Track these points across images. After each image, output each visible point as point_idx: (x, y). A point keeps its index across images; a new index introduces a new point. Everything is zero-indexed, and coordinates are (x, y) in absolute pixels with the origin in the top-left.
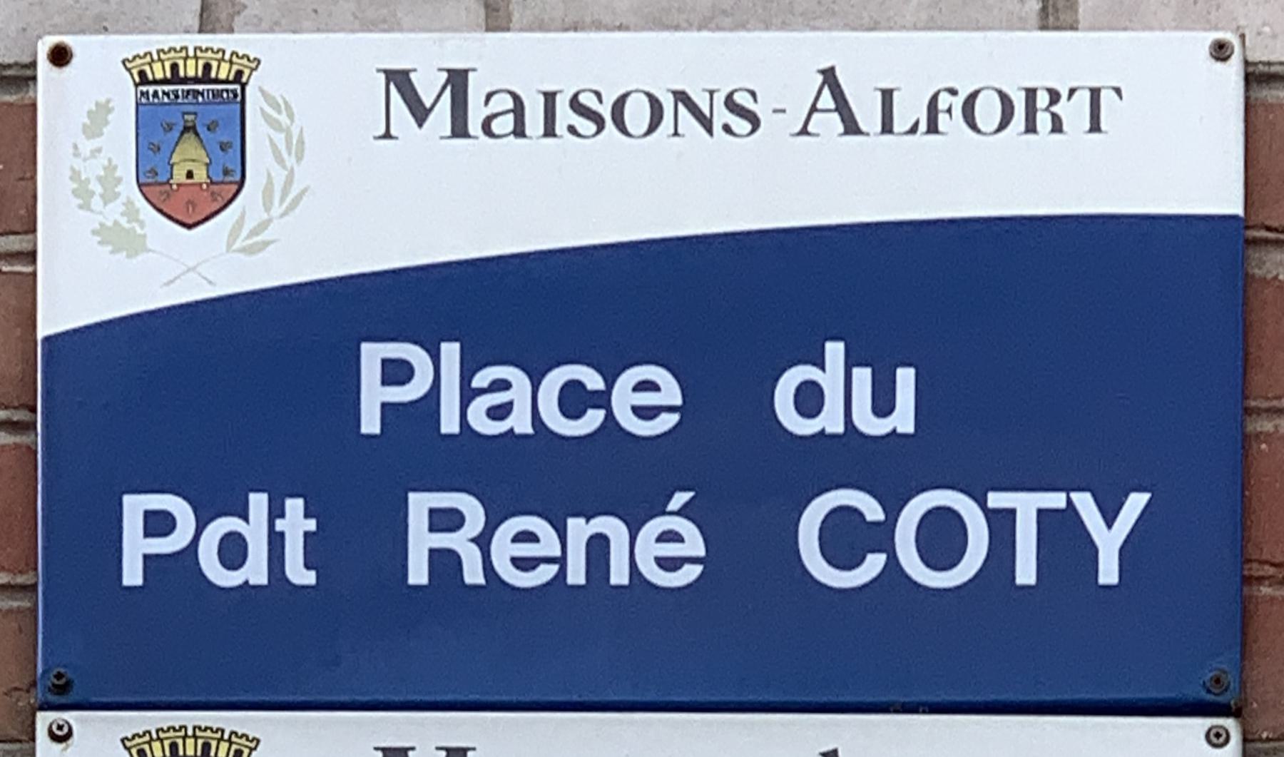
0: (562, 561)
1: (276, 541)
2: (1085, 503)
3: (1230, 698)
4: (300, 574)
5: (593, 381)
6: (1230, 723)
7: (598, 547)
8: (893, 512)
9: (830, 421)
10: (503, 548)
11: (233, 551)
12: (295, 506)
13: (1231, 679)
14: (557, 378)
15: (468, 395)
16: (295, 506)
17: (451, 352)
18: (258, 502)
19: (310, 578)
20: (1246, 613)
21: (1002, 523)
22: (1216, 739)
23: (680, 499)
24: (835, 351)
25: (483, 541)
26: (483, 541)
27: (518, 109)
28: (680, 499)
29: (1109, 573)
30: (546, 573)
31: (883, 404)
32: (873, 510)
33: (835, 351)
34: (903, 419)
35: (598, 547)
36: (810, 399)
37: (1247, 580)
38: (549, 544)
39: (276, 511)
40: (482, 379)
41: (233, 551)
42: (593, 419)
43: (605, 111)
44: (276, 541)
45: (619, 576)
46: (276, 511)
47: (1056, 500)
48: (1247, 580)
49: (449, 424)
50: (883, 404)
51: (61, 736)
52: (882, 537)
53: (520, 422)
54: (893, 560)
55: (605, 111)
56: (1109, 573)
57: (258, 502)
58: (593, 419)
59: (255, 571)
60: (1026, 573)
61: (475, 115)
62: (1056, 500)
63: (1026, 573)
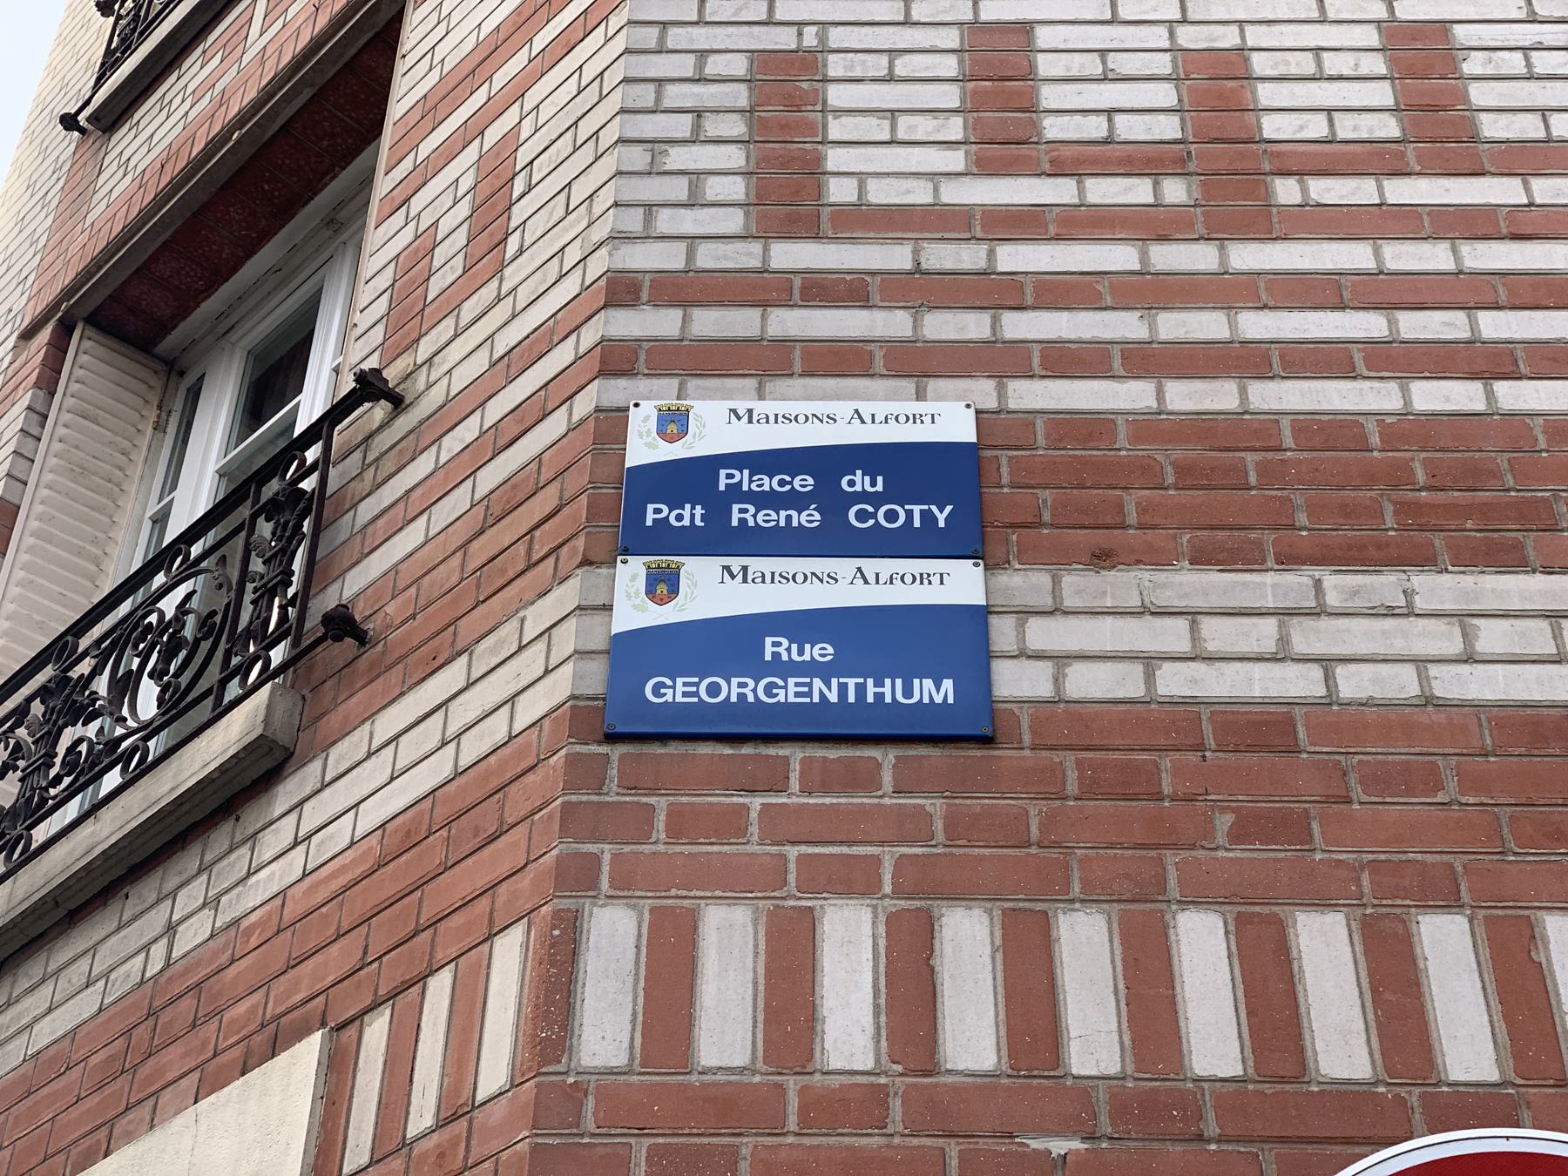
0: (778, 521)
1: (693, 516)
2: (934, 508)
3: (980, 555)
4: (698, 522)
5: (788, 478)
6: (980, 561)
7: (789, 518)
8: (876, 511)
9: (858, 488)
10: (760, 517)
11: (680, 518)
12: (698, 507)
13: (980, 550)
14: (777, 478)
15: (751, 482)
16: (698, 507)
17: (746, 472)
18: (688, 506)
19: (703, 524)
20: (983, 534)
21: (909, 514)
22: (976, 565)
23: (813, 506)
24: (859, 473)
25: (755, 516)
26: (755, 516)
27: (767, 417)
28: (813, 506)
29: (942, 524)
30: (773, 524)
31: (873, 484)
32: (871, 509)
33: (859, 473)
34: (880, 487)
35: (789, 518)
36: (852, 483)
37: (983, 527)
38: (774, 516)
39: (693, 508)
40: (755, 478)
41: (680, 518)
42: (788, 487)
43: (792, 418)
44: (693, 516)
45: (795, 524)
46: (693, 508)
47: (926, 507)
48: (983, 527)
49: (745, 488)
50: (873, 484)
51: (625, 562)
52: (874, 516)
53: (767, 488)
54: (877, 520)
55: (792, 418)
56: (942, 524)
57: (688, 506)
58: (788, 487)
59: (686, 522)
60: (917, 524)
61: (755, 419)
62: (926, 507)
63: (917, 524)
